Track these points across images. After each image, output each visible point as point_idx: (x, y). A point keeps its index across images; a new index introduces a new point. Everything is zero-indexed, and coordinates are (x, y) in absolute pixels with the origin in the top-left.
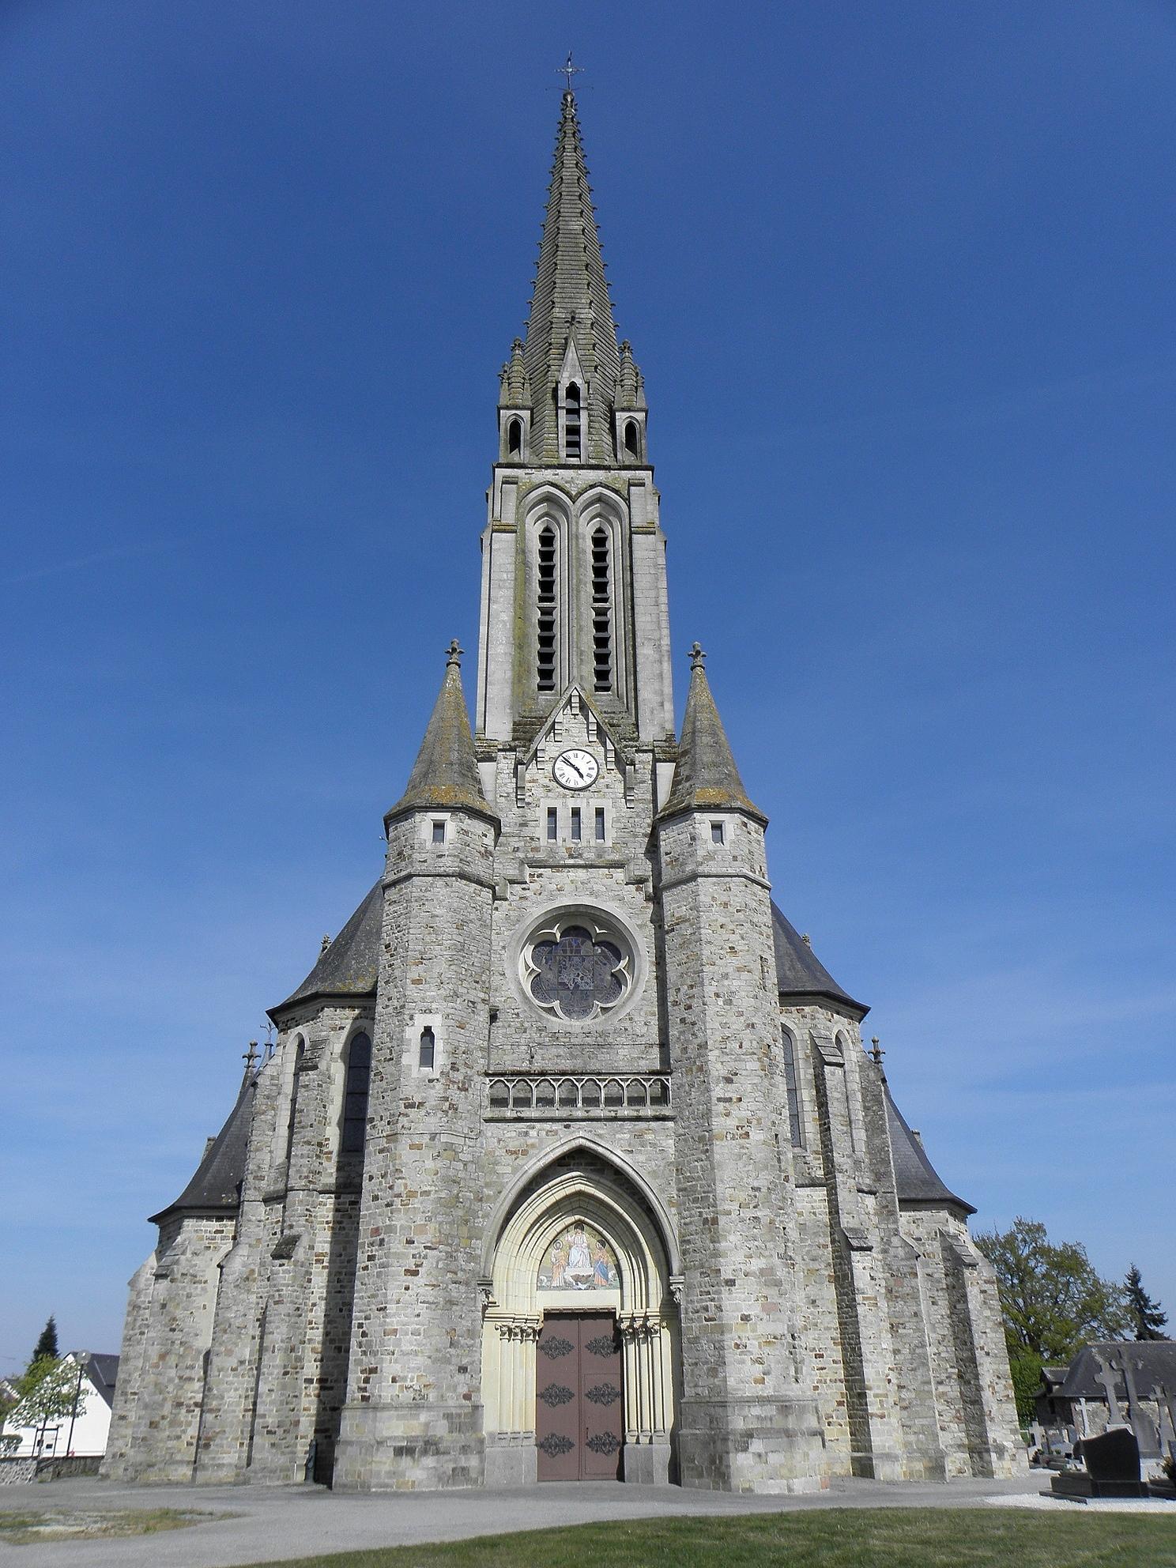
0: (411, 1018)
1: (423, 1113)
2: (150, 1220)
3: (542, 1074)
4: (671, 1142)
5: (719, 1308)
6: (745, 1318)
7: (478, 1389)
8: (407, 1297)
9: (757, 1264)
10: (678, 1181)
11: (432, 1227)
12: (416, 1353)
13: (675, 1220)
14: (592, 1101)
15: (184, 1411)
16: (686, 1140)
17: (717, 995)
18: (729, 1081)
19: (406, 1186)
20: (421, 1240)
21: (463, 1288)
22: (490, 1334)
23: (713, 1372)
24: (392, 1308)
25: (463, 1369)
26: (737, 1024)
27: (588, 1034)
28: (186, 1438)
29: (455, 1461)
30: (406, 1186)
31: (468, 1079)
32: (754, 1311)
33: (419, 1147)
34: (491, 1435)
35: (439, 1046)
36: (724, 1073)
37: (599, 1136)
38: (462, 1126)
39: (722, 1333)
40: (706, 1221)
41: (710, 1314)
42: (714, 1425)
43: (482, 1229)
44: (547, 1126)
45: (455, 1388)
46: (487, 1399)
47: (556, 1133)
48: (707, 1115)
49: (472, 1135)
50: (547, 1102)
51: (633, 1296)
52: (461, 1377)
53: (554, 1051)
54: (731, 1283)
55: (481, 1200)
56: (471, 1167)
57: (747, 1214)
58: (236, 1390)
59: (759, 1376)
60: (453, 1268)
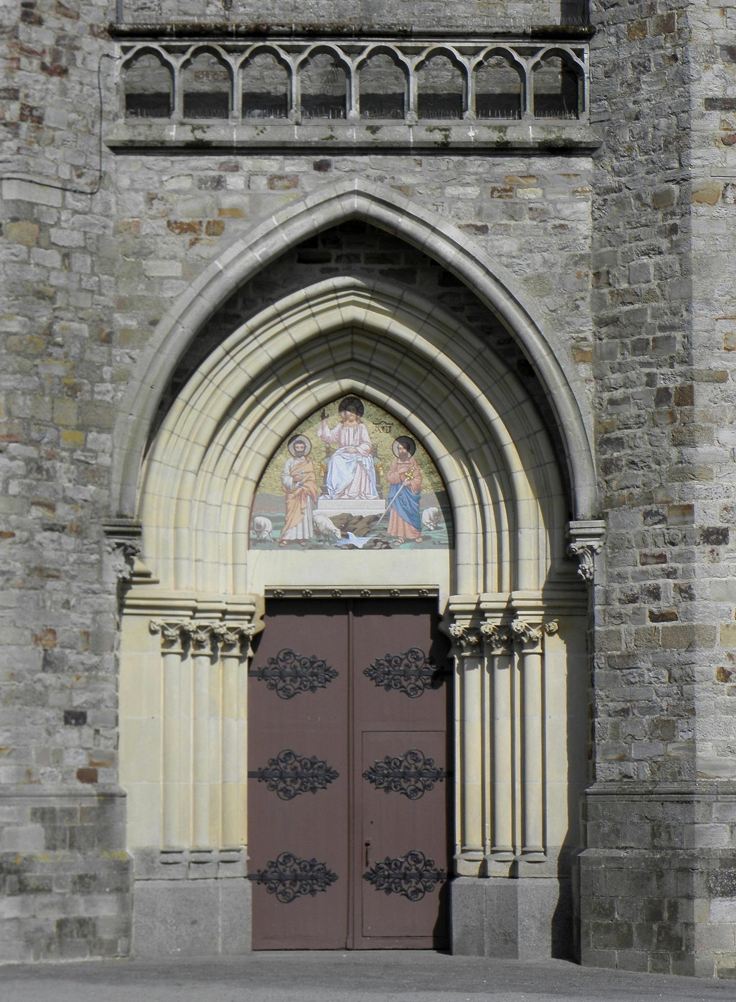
3: (258, 32)
4: (584, 207)
5: (687, 593)
7: (112, 760)
10: (599, 303)
13: (587, 393)
14: (383, 105)
16: (621, 204)
21: (69, 542)
22: (137, 647)
23: (665, 729)
25: (75, 718)
29: (63, 906)
31: (67, 44)
34: (146, 855)
37: (404, 190)
38: (55, 160)
39: (690, 647)
40: (663, 396)
41: (663, 605)
42: (663, 841)
43: (111, 408)
44: (272, 164)
45: (58, 756)
46: (132, 777)
47: (293, 181)
49: (82, 183)
50: (269, 103)
51: (484, 562)
52: (71, 735)
55: (107, 340)
56: (82, 262)
60: (44, 493)
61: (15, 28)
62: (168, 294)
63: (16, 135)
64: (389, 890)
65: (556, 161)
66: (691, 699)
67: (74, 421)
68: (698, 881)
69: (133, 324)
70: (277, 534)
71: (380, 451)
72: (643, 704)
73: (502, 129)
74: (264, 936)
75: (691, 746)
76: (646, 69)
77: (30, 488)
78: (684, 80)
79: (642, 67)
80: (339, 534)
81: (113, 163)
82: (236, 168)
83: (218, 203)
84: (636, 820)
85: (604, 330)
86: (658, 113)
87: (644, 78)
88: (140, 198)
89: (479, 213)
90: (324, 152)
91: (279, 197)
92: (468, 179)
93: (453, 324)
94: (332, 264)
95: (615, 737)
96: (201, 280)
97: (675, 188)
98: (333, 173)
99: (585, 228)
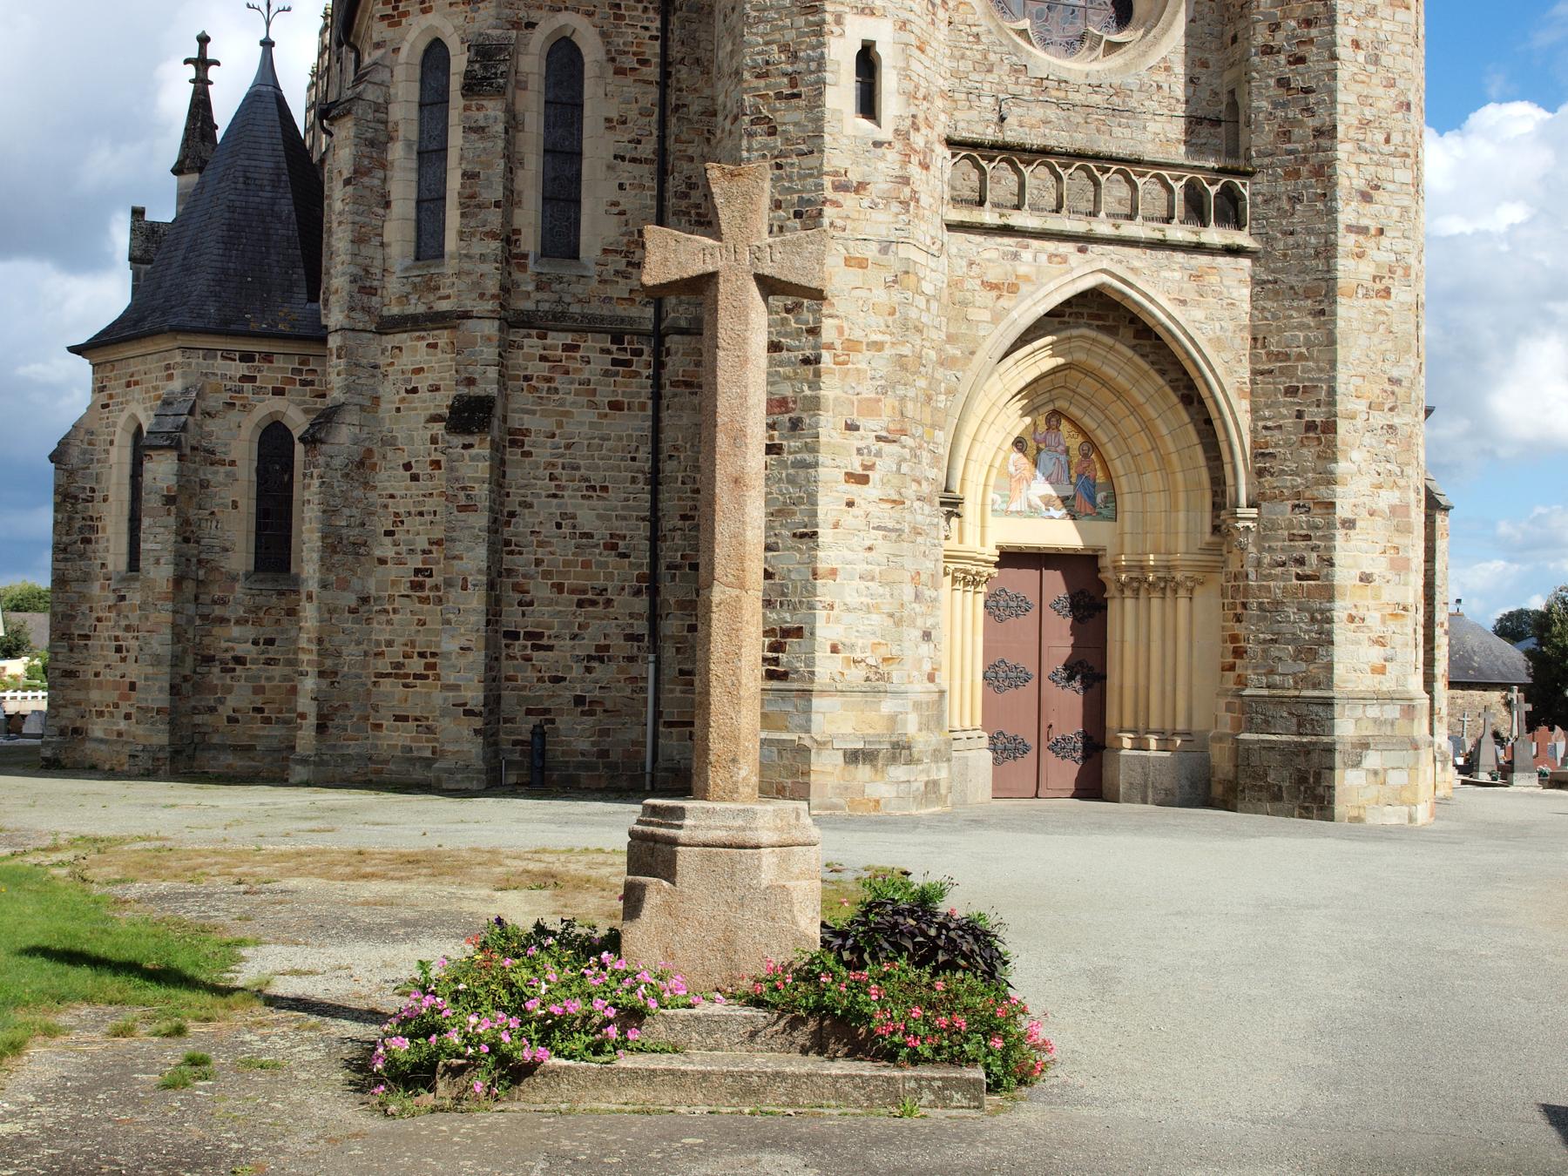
0: (839, 20)
1: (866, 203)
2: (76, 350)
4: (1246, 292)
6: (1366, 578)
8: (849, 518)
9: (1387, 498)
10: (1254, 358)
11: (889, 402)
12: (869, 609)
13: (1245, 420)
15: (216, 670)
16: (1277, 293)
17: (1356, 44)
18: (1366, 197)
19: (840, 330)
20: (872, 425)
26: (1386, 102)
27: (1096, 88)
28: (225, 711)
30: (840, 330)
32: (1378, 566)
33: (862, 264)
35: (889, 81)
36: (1359, 183)
39: (1331, 599)
40: (1311, 427)
41: (1308, 570)
44: (1051, 246)
48: (1328, 251)
53: (1038, 112)
54: (1349, 524)
57: (1379, 419)
58: (359, 643)
59: (1379, 662)
61: (908, 133)
62: (982, 333)
64: (1064, 757)
65: (1228, 259)
66: (1330, 633)
67: (929, 422)
68: (1338, 757)
69: (958, 353)
70: (1004, 506)
73: (1196, 233)
74: (1001, 790)
75: (1329, 667)
77: (912, 469)
78: (1332, 212)
79: (1295, 200)
81: (947, 236)
82: (1027, 247)
83: (1015, 271)
85: (1259, 378)
86: (1310, 231)
88: (964, 263)
89: (1181, 290)
90: (1085, 240)
91: (1055, 268)
93: (1146, 366)
96: (1003, 325)
97: (1323, 284)
98: (1089, 255)
99: (1247, 307)
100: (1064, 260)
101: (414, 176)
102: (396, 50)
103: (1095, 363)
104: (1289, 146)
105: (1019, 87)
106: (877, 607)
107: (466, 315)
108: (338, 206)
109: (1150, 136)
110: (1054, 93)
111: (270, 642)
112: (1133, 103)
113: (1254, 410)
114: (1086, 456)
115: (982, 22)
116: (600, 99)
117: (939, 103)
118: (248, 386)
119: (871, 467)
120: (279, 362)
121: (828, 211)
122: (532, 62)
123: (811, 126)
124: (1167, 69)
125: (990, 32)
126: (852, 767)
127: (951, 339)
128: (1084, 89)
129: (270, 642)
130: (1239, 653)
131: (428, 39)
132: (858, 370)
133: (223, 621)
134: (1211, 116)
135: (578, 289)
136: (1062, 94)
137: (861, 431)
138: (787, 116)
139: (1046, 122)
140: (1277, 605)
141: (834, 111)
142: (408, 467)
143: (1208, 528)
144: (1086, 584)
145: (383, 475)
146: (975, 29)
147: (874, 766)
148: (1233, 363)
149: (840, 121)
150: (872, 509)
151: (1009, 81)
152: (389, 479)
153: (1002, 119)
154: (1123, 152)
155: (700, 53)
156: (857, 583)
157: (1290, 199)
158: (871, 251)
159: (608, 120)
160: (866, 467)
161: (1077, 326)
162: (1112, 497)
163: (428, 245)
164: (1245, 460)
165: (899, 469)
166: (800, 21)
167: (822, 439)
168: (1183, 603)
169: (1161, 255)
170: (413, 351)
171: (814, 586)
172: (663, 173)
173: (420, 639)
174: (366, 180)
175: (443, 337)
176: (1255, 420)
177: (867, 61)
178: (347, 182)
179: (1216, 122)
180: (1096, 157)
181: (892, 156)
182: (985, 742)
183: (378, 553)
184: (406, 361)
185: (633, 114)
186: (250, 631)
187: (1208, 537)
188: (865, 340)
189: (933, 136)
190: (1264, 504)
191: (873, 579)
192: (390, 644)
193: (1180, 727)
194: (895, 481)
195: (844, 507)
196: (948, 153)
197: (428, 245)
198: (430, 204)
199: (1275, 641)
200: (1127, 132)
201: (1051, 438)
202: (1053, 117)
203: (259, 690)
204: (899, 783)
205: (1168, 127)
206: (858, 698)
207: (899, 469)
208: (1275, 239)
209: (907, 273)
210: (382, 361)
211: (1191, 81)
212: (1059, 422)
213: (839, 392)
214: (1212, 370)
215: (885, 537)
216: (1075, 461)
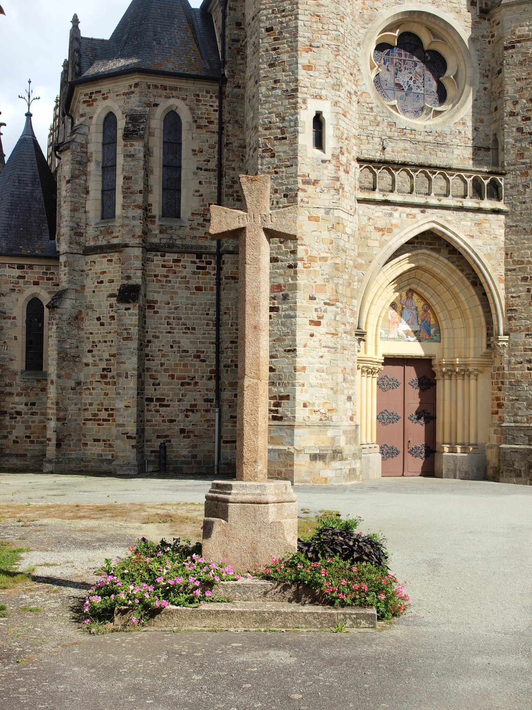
0: (304, 101)
1: (318, 190)
4: (502, 231)
8: (312, 342)
10: (506, 263)
11: (330, 286)
12: (321, 386)
15: (7, 418)
19: (306, 252)
20: (322, 297)
24: (300, 350)
27: (429, 133)
28: (12, 437)
30: (306, 252)
33: (316, 219)
35: (329, 131)
44: (408, 210)
58: (76, 404)
61: (338, 156)
62: (375, 252)
63: (338, 194)
64: (416, 457)
65: (494, 216)
67: (349, 295)
69: (363, 262)
70: (386, 336)
71: (418, 309)
72: (524, 397)
73: (478, 203)
74: (385, 473)
76: (528, 187)
77: (342, 318)
80: (405, 336)
81: (358, 205)
82: (396, 210)
84: (522, 435)
85: (509, 273)
87: (527, 190)
88: (366, 218)
89: (471, 231)
91: (410, 220)
92: (468, 219)
93: (454, 267)
94: (415, 245)
95: (512, 408)
96: (385, 249)
98: (426, 214)
99: (503, 238)
100: (414, 216)
101: (100, 179)
102: (91, 118)
103: (430, 266)
104: (523, 161)
105: (392, 133)
106: (325, 385)
107: (126, 246)
108: (64, 193)
109: (456, 156)
110: (409, 136)
111: (33, 404)
112: (447, 140)
113: (507, 288)
114: (425, 311)
115: (374, 101)
116: (189, 140)
117: (353, 141)
118: (21, 281)
119: (322, 318)
120: (36, 269)
121: (300, 194)
122: (156, 123)
123: (291, 153)
124: (464, 124)
125: (378, 106)
126: (314, 462)
127: (360, 255)
128: (424, 134)
129: (33, 404)
130: (500, 406)
131: (106, 113)
132: (315, 271)
133: (10, 394)
134: (485, 146)
135: (180, 232)
136: (413, 136)
137: (317, 300)
138: (280, 148)
139: (405, 150)
140: (518, 382)
141: (303, 146)
142: (99, 319)
143: (484, 345)
144: (426, 373)
145: (87, 323)
146: (370, 105)
147: (324, 462)
148: (496, 266)
149: (306, 150)
150: (323, 338)
151: (387, 130)
152: (90, 325)
153: (384, 149)
154: (442, 164)
155: (238, 118)
156: (315, 373)
157: (523, 186)
158: (321, 213)
159: (194, 151)
160: (319, 318)
161: (421, 248)
162: (438, 331)
163: (107, 211)
164: (502, 312)
165: (335, 318)
166: (286, 102)
167: (298, 304)
168: (473, 382)
169: (461, 214)
170: (100, 263)
171: (295, 375)
172: (220, 176)
173: (106, 402)
174: (77, 181)
175: (115, 256)
176: (507, 293)
177: (318, 121)
178: (68, 182)
179: (487, 149)
180: (429, 167)
181: (331, 167)
182: (378, 449)
183: (85, 361)
184: (97, 268)
185: (205, 148)
186: (24, 399)
187: (484, 350)
188: (318, 256)
189: (351, 157)
190: (512, 334)
191: (323, 371)
192: (91, 404)
193: (472, 441)
194: (334, 324)
195: (309, 337)
196: (358, 165)
197: (107, 211)
198: (108, 192)
199: (517, 400)
200: (444, 154)
201: (409, 303)
202: (408, 148)
203: (28, 428)
204: (336, 470)
205: (464, 152)
206: (316, 429)
207: (335, 318)
208: (516, 205)
209: (338, 223)
210: (86, 268)
211: (475, 129)
212: (412, 295)
213: (306, 282)
214: (486, 269)
215: (329, 351)
216: (420, 313)
